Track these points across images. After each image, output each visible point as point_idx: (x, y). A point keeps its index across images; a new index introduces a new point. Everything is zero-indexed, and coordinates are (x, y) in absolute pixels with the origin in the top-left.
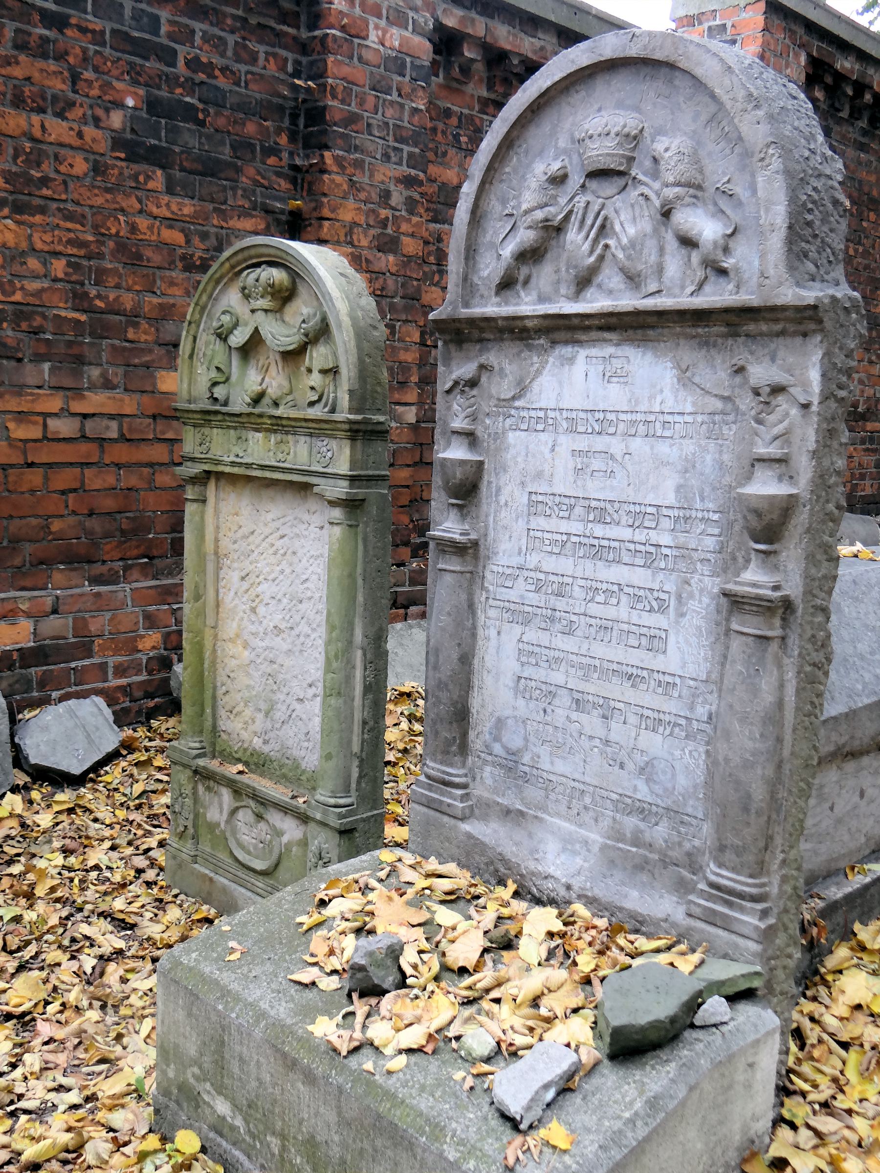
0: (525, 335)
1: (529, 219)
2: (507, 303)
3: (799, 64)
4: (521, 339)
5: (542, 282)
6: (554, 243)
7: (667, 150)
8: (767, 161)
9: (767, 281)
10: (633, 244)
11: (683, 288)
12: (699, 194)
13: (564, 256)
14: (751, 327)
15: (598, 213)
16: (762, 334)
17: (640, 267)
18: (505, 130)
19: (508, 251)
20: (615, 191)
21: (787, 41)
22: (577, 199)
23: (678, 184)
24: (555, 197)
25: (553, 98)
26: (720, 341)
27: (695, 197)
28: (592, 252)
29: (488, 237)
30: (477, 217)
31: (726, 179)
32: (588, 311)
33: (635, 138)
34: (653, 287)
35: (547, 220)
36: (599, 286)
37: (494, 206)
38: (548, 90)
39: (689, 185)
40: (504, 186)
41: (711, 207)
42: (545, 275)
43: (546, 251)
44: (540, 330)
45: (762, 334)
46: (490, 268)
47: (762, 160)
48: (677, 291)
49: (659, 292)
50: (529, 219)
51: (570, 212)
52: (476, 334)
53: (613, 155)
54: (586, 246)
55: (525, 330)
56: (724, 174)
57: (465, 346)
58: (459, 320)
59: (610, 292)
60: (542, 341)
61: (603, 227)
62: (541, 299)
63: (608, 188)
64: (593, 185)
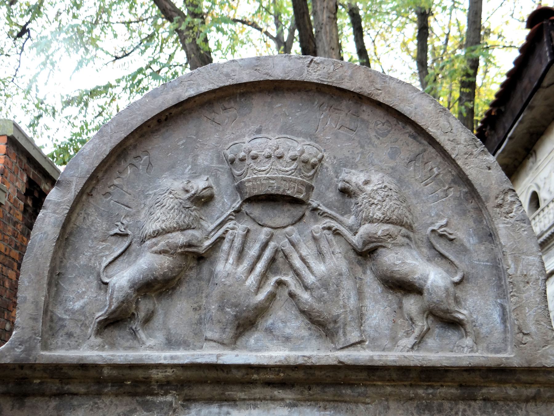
0: (142, 388)
1: (162, 242)
2: (113, 346)
3: (23, 180)
4: (133, 395)
5: (172, 322)
6: (193, 274)
7: (367, 183)
8: (506, 208)
9: (526, 339)
10: (324, 283)
11: (394, 340)
12: (411, 234)
13: (216, 292)
14: (493, 390)
15: (265, 246)
16: (506, 399)
17: (336, 311)
18: (123, 135)
19: (123, 278)
20: (289, 221)
21: (17, 164)
22: (230, 225)
23: (388, 221)
24: (198, 219)
25: (191, 111)
26: (447, 405)
27: (408, 237)
28: (259, 288)
29: (83, 260)
30: (67, 235)
31: (444, 222)
32: (265, 362)
33: (314, 166)
34: (354, 337)
35: (190, 245)
36: (269, 331)
37: (94, 221)
38: (189, 99)
39: (400, 223)
40: (112, 201)
41: (425, 250)
42: (177, 312)
43: (180, 283)
44: (168, 383)
45: (506, 399)
46: (83, 300)
47: (500, 206)
48: (386, 342)
49: (361, 342)
50: (162, 242)
51: (221, 239)
52: (54, 386)
53: (291, 180)
54: (252, 280)
55: (147, 381)
56: (440, 217)
57: (29, 402)
58: (32, 367)
59: (287, 339)
60: (169, 398)
61: (273, 260)
62: (171, 343)
63: (280, 216)
64: (256, 211)
